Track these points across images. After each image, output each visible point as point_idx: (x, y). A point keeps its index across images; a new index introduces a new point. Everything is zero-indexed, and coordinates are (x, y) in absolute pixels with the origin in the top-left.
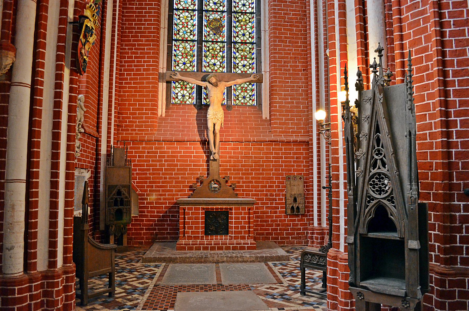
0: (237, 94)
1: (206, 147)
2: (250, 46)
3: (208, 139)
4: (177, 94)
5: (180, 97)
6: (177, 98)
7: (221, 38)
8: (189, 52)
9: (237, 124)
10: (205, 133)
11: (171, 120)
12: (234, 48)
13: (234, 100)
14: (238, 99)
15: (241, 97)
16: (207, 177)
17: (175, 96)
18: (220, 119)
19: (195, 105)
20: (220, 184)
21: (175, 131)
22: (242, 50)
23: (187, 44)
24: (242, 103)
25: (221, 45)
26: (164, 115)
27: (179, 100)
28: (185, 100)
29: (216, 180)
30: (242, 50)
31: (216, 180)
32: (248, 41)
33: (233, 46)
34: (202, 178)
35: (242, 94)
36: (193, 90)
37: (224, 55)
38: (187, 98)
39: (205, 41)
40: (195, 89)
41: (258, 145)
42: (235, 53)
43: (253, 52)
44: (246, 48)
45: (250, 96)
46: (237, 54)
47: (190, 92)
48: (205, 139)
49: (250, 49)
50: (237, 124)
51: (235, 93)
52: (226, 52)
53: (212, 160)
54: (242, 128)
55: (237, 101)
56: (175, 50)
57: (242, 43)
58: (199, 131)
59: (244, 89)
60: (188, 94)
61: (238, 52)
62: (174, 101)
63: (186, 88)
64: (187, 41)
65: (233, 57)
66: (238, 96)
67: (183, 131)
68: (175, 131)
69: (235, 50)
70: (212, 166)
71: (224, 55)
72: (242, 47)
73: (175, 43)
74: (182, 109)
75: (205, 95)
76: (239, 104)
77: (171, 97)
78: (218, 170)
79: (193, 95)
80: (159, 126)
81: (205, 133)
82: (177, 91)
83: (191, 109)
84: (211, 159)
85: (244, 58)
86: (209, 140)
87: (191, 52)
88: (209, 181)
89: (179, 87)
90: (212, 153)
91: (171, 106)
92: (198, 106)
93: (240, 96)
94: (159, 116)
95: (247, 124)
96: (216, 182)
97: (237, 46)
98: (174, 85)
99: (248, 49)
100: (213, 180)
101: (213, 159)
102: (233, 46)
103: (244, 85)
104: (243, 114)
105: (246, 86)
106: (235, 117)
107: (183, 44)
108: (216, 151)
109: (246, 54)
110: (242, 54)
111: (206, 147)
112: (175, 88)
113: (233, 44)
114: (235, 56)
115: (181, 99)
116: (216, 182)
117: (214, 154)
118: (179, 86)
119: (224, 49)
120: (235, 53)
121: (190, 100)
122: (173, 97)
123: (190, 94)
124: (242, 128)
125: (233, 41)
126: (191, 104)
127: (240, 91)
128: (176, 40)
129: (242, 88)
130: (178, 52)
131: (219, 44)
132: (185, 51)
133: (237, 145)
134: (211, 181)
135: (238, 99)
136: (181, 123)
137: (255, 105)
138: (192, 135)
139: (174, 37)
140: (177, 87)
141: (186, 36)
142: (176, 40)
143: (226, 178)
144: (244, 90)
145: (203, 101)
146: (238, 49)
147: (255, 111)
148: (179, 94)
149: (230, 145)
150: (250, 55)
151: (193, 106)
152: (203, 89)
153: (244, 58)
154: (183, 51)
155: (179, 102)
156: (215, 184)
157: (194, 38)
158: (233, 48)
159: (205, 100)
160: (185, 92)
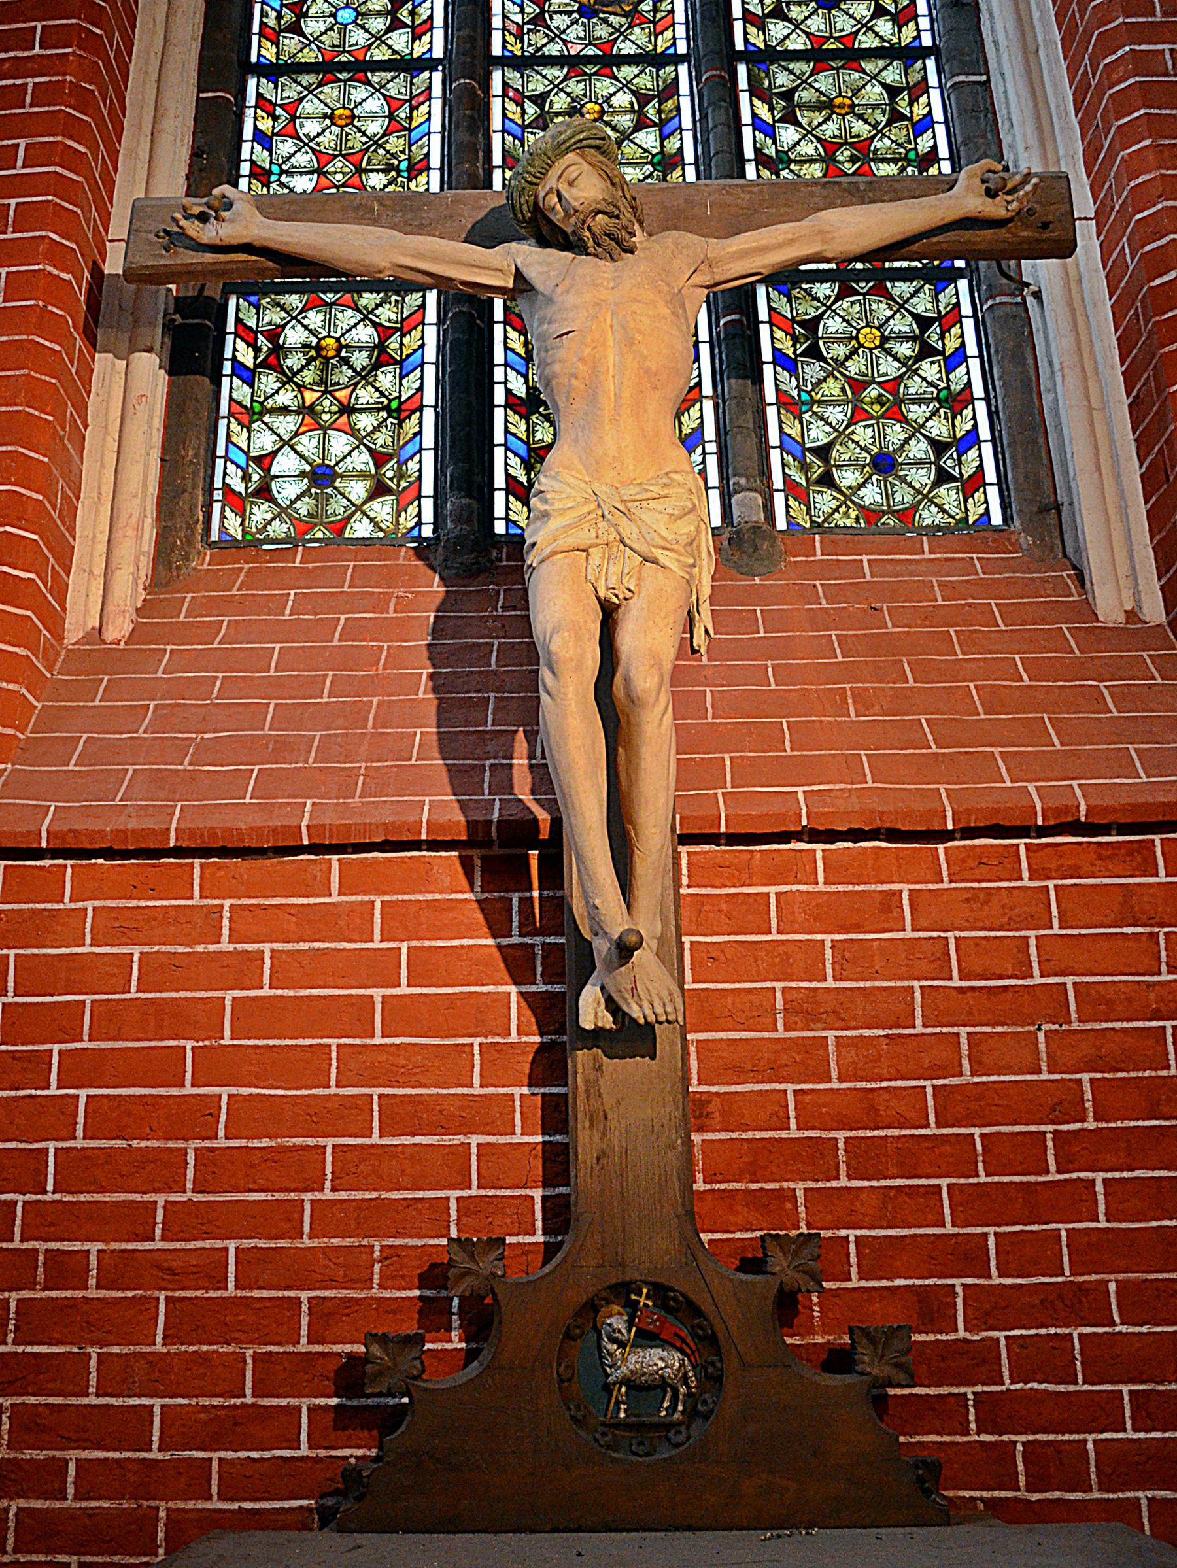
0: (818, 434)
1: (527, 903)
2: (893, 75)
3: (542, 815)
4: (265, 461)
5: (287, 491)
6: (264, 492)
7: (639, 35)
8: (376, 142)
9: (848, 672)
10: (520, 762)
11: (181, 661)
12: (755, 91)
13: (790, 487)
14: (827, 480)
15: (855, 464)
16: (550, 1250)
17: (246, 478)
18: (664, 557)
19: (423, 549)
20: (711, 1341)
21: (205, 752)
22: (826, 105)
23: (359, 93)
24: (870, 514)
25: (645, 81)
26: (119, 629)
27: (284, 512)
28: (337, 507)
29: (659, 1291)
30: (826, 105)
31: (659, 1291)
32: (867, 41)
33: (743, 83)
34: (487, 1264)
35: (863, 434)
36: (411, 426)
37: (672, 145)
38: (358, 490)
39: (506, 61)
40: (429, 416)
41: (1108, 857)
42: (770, 132)
43: (919, 111)
44: (856, 92)
45: (939, 447)
46: (788, 135)
47: (382, 439)
48: (514, 813)
49: (893, 91)
50: (848, 672)
51: (794, 431)
52: (687, 122)
53: (596, 1037)
54: (902, 701)
55: (825, 501)
56: (260, 137)
57: (818, 56)
58: (446, 744)
59: (873, 392)
60: (362, 460)
61: (790, 118)
62: (233, 524)
63: (348, 409)
64: (361, 69)
65: (749, 153)
66: (823, 452)
67: (282, 749)
68: (205, 752)
69: (763, 111)
70: (599, 1118)
71: (672, 145)
72: (824, 82)
73: (267, 89)
74: (307, 577)
75: (514, 461)
76: (839, 519)
77: (210, 489)
78: (673, 1159)
79: (413, 465)
80: (49, 719)
81: (520, 762)
82: (264, 442)
83: (389, 577)
84: (587, 1023)
85: (853, 160)
86: (557, 823)
87: (395, 143)
88: (576, 1297)
89: (284, 410)
90: (602, 947)
91: (204, 561)
92: (456, 546)
93: (841, 454)
94: (73, 633)
95: (952, 671)
96: (652, 1320)
97: (783, 80)
98: (243, 393)
99: (874, 92)
100: (622, 1292)
101: (607, 1021)
102: (743, 83)
103: (873, 362)
104: (892, 591)
105: (889, 368)
106: (817, 620)
107: (331, 92)
108: (648, 924)
109: (861, 128)
110: (831, 129)
111: (527, 903)
112: (249, 415)
113: (742, 70)
114: (771, 151)
115: (303, 507)
116: (652, 1320)
117: (625, 950)
118: (286, 398)
119: (670, 104)
120: (770, 132)
121: (382, 509)
122: (227, 488)
123: (380, 459)
124: (902, 701)
125: (739, 45)
126: (387, 543)
127: (836, 415)
128: (271, 72)
129: (858, 385)
130: (285, 147)
131: (627, 72)
132: (343, 138)
133: (877, 869)
134: (591, 1309)
135: (827, 480)
136: (276, 687)
137: (997, 519)
138: (378, 783)
139: (261, 51)
140: (264, 411)
141: (359, 38)
142: (271, 72)
143: (778, 1262)
144: (879, 400)
145: (499, 511)
146: (788, 95)
147: (1006, 566)
148: (286, 463)
149: (803, 869)
150: (898, 132)
151: (404, 557)
152: (499, 414)
153: (853, 160)
154: (328, 141)
155: (279, 529)
156: (646, 1338)
157: (419, 49)
158: (744, 98)
159: (516, 505)
160: (339, 443)
